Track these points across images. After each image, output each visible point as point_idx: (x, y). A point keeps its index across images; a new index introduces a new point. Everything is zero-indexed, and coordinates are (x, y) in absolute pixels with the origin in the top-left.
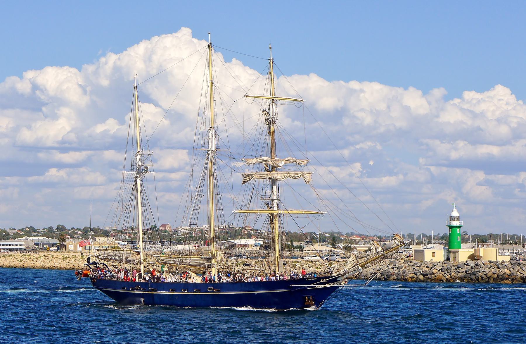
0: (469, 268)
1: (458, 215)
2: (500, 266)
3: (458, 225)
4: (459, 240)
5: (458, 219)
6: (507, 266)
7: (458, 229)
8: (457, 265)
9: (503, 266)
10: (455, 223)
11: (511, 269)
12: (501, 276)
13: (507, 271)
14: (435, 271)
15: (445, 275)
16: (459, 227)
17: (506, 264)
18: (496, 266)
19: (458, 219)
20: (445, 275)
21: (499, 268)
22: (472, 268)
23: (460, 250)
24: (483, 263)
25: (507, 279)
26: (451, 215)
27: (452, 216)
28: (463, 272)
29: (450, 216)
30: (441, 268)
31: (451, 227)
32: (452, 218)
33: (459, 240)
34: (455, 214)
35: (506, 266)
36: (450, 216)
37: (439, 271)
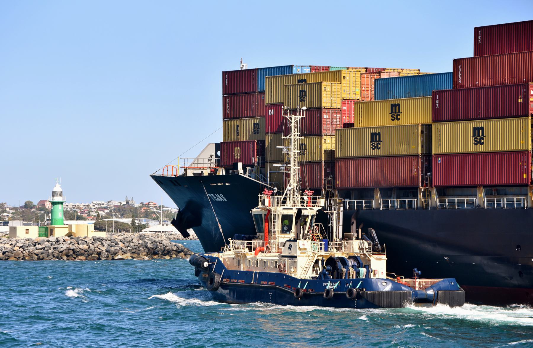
0: (49, 244)
1: (61, 191)
2: (80, 242)
3: (61, 201)
4: (61, 216)
5: (61, 194)
6: (87, 242)
7: (60, 205)
8: (38, 242)
9: (83, 242)
10: (57, 199)
11: (91, 245)
12: (78, 252)
13: (85, 247)
14: (16, 248)
15: (24, 252)
16: (61, 203)
17: (86, 240)
18: (76, 242)
19: (61, 194)
20: (24, 252)
21: (78, 244)
22: (52, 245)
23: (56, 226)
24: (64, 240)
25: (82, 255)
26: (54, 190)
27: (55, 192)
28: (41, 249)
29: (53, 192)
30: (21, 245)
31: (54, 203)
32: (54, 194)
33: (61, 216)
34: (58, 189)
35: (86, 242)
36: (53, 192)
37: (20, 248)
